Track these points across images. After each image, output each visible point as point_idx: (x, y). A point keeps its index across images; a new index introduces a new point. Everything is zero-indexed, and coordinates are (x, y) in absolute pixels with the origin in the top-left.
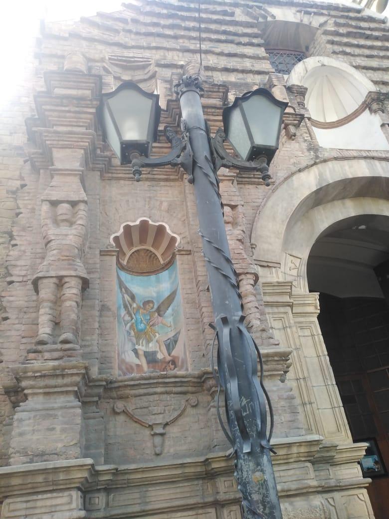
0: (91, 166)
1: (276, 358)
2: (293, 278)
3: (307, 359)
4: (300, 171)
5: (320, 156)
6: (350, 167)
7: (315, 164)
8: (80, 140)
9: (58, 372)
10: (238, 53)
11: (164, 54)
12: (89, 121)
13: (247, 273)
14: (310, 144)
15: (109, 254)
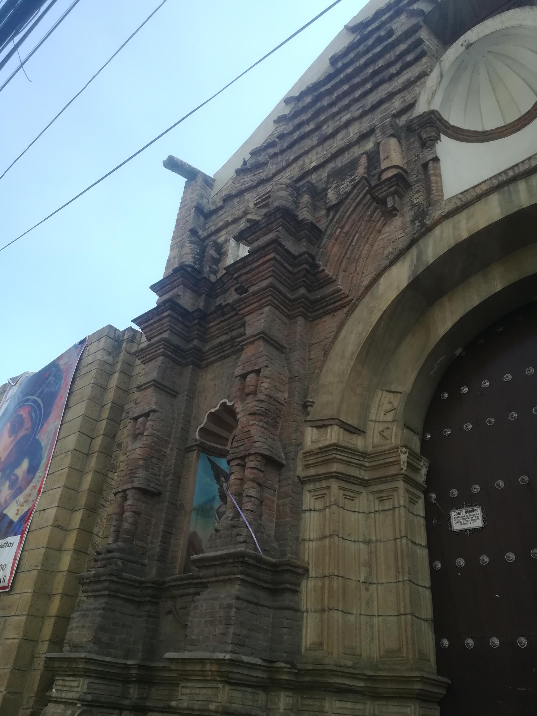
0: (184, 362)
1: (230, 561)
2: (386, 425)
3: (378, 543)
4: (392, 263)
5: (427, 222)
6: (468, 219)
7: (413, 242)
8: (157, 349)
9: (97, 579)
10: (383, 96)
11: (304, 161)
12: (169, 323)
13: (250, 455)
14: (419, 208)
15: (192, 449)
